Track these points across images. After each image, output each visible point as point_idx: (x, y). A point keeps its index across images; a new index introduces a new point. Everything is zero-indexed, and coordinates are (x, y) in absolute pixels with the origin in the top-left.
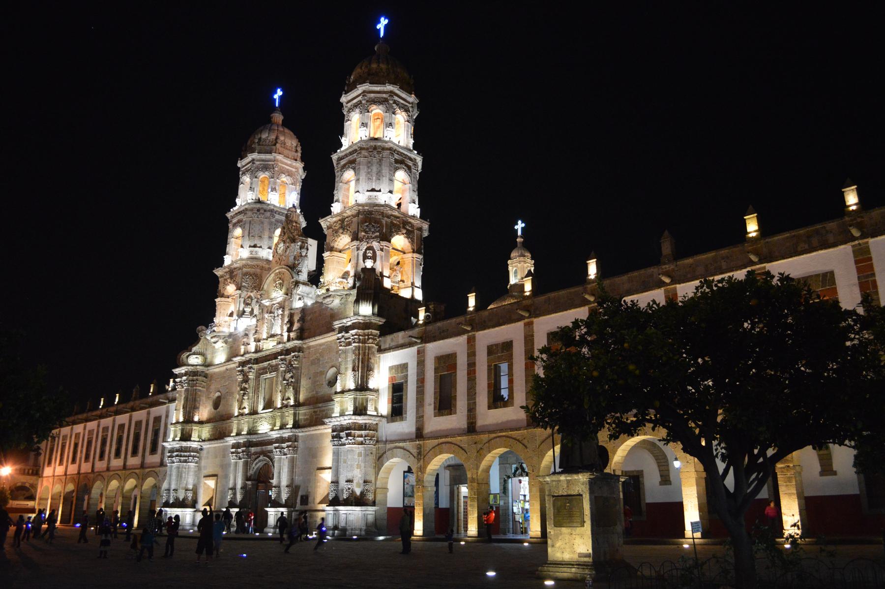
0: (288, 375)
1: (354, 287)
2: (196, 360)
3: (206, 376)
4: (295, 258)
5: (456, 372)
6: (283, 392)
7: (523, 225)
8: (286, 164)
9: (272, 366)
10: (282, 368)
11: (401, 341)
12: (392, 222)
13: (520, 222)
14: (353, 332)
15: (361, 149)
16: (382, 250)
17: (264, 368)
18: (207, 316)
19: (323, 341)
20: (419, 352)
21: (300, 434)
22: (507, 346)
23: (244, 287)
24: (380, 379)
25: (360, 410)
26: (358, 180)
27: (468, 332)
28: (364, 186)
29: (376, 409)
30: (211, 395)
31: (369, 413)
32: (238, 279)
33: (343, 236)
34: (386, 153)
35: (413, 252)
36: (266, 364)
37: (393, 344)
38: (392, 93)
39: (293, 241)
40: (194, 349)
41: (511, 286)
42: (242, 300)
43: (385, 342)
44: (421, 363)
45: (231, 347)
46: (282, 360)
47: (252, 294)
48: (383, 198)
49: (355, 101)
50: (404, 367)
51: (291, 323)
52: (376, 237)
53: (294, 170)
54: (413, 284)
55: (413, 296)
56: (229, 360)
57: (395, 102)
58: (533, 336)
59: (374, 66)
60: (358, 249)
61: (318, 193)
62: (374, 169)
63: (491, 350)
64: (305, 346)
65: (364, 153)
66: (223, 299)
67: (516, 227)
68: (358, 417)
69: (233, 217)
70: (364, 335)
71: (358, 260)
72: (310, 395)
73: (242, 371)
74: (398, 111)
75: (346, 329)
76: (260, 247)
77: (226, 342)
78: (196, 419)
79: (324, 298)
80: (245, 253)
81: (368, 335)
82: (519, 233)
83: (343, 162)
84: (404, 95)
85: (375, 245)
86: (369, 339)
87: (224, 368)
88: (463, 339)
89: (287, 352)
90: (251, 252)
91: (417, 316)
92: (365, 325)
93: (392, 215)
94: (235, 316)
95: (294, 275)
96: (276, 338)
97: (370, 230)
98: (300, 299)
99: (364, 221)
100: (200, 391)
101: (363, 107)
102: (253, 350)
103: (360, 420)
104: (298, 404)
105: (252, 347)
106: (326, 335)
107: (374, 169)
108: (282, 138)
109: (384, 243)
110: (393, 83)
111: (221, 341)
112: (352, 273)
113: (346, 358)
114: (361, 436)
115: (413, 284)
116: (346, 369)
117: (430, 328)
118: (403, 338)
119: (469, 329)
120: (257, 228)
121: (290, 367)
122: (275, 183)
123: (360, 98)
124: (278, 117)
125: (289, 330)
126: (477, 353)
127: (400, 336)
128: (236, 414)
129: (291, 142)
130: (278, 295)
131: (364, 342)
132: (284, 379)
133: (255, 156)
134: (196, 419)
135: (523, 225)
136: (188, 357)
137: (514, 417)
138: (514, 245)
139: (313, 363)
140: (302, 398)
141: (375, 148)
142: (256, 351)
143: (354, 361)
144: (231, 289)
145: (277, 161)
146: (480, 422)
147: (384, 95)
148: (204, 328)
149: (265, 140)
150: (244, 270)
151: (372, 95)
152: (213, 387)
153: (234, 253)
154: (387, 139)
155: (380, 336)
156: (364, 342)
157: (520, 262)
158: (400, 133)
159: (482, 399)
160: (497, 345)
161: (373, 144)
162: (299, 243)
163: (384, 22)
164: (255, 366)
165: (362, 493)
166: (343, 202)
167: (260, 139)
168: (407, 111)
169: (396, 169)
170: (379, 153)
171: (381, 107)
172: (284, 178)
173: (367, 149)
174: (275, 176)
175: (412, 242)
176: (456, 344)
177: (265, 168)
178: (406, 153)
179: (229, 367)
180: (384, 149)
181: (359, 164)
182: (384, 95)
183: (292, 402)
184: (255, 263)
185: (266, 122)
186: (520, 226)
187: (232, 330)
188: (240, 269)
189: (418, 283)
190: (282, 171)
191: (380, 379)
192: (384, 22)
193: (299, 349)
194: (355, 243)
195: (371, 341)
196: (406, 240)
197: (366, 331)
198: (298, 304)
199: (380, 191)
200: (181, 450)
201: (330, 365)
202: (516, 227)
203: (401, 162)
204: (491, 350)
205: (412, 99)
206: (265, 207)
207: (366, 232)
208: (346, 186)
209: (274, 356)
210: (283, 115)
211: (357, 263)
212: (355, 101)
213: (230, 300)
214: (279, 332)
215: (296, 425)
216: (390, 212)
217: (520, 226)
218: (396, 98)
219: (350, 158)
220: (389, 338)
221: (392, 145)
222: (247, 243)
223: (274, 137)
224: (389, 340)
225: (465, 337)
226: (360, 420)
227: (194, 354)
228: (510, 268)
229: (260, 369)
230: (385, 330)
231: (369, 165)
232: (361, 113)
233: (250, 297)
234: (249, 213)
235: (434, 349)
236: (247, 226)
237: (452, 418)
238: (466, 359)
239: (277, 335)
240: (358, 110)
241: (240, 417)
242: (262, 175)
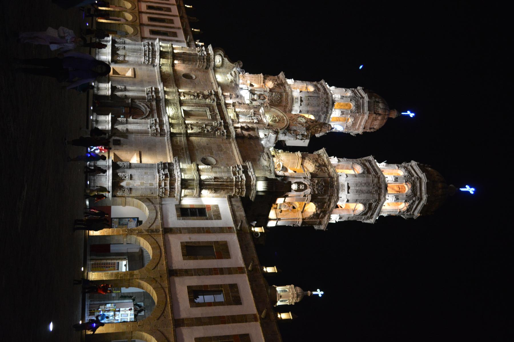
0: (209, 128)
1: (277, 176)
2: (218, 61)
3: (207, 68)
4: (295, 130)
5: (216, 259)
6: (197, 125)
7: (320, 296)
8: (360, 123)
9: (215, 116)
10: (214, 124)
11: (237, 214)
12: (325, 202)
13: (322, 293)
14: (244, 177)
15: (379, 178)
16: (305, 196)
17: (214, 110)
18: (250, 68)
19: (235, 153)
20: (230, 228)
21: (166, 138)
22: (237, 301)
23: (272, 94)
24: (209, 199)
25: (185, 184)
26: (355, 176)
27: (247, 267)
28: (352, 181)
29: (185, 196)
30: (193, 72)
31: (183, 190)
32: (277, 90)
33: (314, 166)
34: (376, 196)
35: (303, 219)
36: (217, 111)
37: (235, 207)
38: (420, 199)
39: (308, 129)
40: (226, 60)
41: (275, 288)
42: (262, 93)
43: (236, 201)
44: (221, 230)
45: (228, 86)
46: (221, 123)
47: (266, 100)
48: (343, 195)
49: (413, 172)
50: (218, 217)
51: (248, 129)
52: (314, 191)
53: (357, 127)
54: (279, 219)
55: (271, 220)
56: (219, 84)
57: (414, 202)
58: (246, 322)
59: (440, 185)
60: (305, 178)
61: (344, 146)
62: (365, 188)
63: (234, 287)
64: (231, 140)
65: (376, 180)
66: (262, 79)
67: (318, 290)
68: (179, 182)
69: (321, 84)
70: (242, 185)
71: (297, 178)
72: (195, 145)
73: (211, 94)
74: (407, 204)
75: (245, 172)
76: (301, 105)
77: (232, 82)
78: (176, 62)
79: (267, 154)
80: (296, 94)
81: (241, 188)
82: (314, 293)
83: (367, 164)
84: (419, 208)
85: (308, 191)
86: (239, 189)
87: (213, 81)
88: (241, 263)
89: (226, 127)
90: (297, 98)
91: (257, 226)
92: (249, 186)
93: (330, 202)
94: (250, 88)
95: (283, 131)
97: (319, 187)
98: (265, 135)
99: (325, 181)
100: (196, 64)
101: (409, 178)
102: (227, 102)
103: (178, 184)
104: (188, 136)
105: (229, 101)
106: (240, 155)
107: (365, 188)
108: (380, 118)
109: (310, 197)
110: (428, 199)
111: (232, 78)
112: (286, 174)
113: (224, 172)
114: (165, 185)
115: (279, 219)
116: (216, 172)
117: (249, 236)
118: (240, 215)
119: (250, 268)
120: (315, 102)
121: (215, 129)
122: (347, 114)
123: (415, 175)
124: (394, 115)
125: (242, 128)
126: (231, 275)
127: (241, 213)
128: (180, 90)
129: (377, 125)
130: (267, 119)
131: (236, 185)
132: (206, 125)
133: (366, 99)
134: (176, 62)
135: (320, 296)
136: (220, 55)
137: (182, 308)
138: (305, 289)
139: (219, 146)
140: (193, 139)
141: (380, 188)
142: (227, 105)
143: (222, 178)
144: (270, 84)
145: (363, 115)
146: (177, 280)
147: (418, 193)
148: (241, 66)
149: (378, 106)
150: (284, 94)
151: (418, 185)
152: (199, 73)
153: (296, 86)
154: (387, 197)
155: (241, 197)
156: (236, 185)
157: (293, 294)
158: (391, 206)
159: (195, 281)
160: (238, 292)
161: (383, 186)
162: (306, 133)
163: (471, 190)
164: (215, 104)
165: (122, 187)
166: (338, 165)
167: (378, 102)
168: (408, 210)
169: (365, 205)
170: (376, 191)
171: (410, 191)
172: (351, 120)
173: (379, 182)
174: (353, 114)
175: (310, 218)
176: (237, 258)
177: (359, 107)
178: (377, 211)
179: (214, 84)
180: (379, 195)
181: (368, 177)
182: (418, 193)
183: (189, 131)
184: (290, 101)
185: (390, 106)
186: (319, 293)
187: (241, 86)
188: (285, 91)
189: (280, 223)
190: (356, 119)
191: (209, 199)
192: (471, 190)
193: (229, 135)
194: (309, 176)
195: (237, 190)
196: (312, 213)
197: (245, 187)
198: (261, 134)
199: (348, 193)
200: (154, 52)
201: (218, 159)
202: (318, 290)
203: (371, 207)
204: (234, 287)
205: (417, 214)
206: (330, 107)
207: (317, 184)
208: (350, 167)
209: (223, 117)
210: (396, 118)
211: (294, 178)
212: (413, 172)
213: (262, 84)
214: (241, 120)
215: (172, 135)
216: (333, 201)
217: (319, 293)
218: (417, 202)
219: (371, 170)
220: (239, 204)
221: (382, 200)
222: (303, 95)
223: (380, 111)
224: (238, 204)
225: (243, 265)
226: (178, 184)
227: (223, 60)
228: (288, 287)
229: (213, 107)
230: (246, 202)
231: (367, 184)
232: (405, 177)
233: (265, 98)
234: (325, 96)
235: (233, 240)
236: (316, 95)
237: (181, 257)
238: (226, 267)
239: (238, 119)
240: (406, 174)
241: (177, 93)
242: (352, 105)
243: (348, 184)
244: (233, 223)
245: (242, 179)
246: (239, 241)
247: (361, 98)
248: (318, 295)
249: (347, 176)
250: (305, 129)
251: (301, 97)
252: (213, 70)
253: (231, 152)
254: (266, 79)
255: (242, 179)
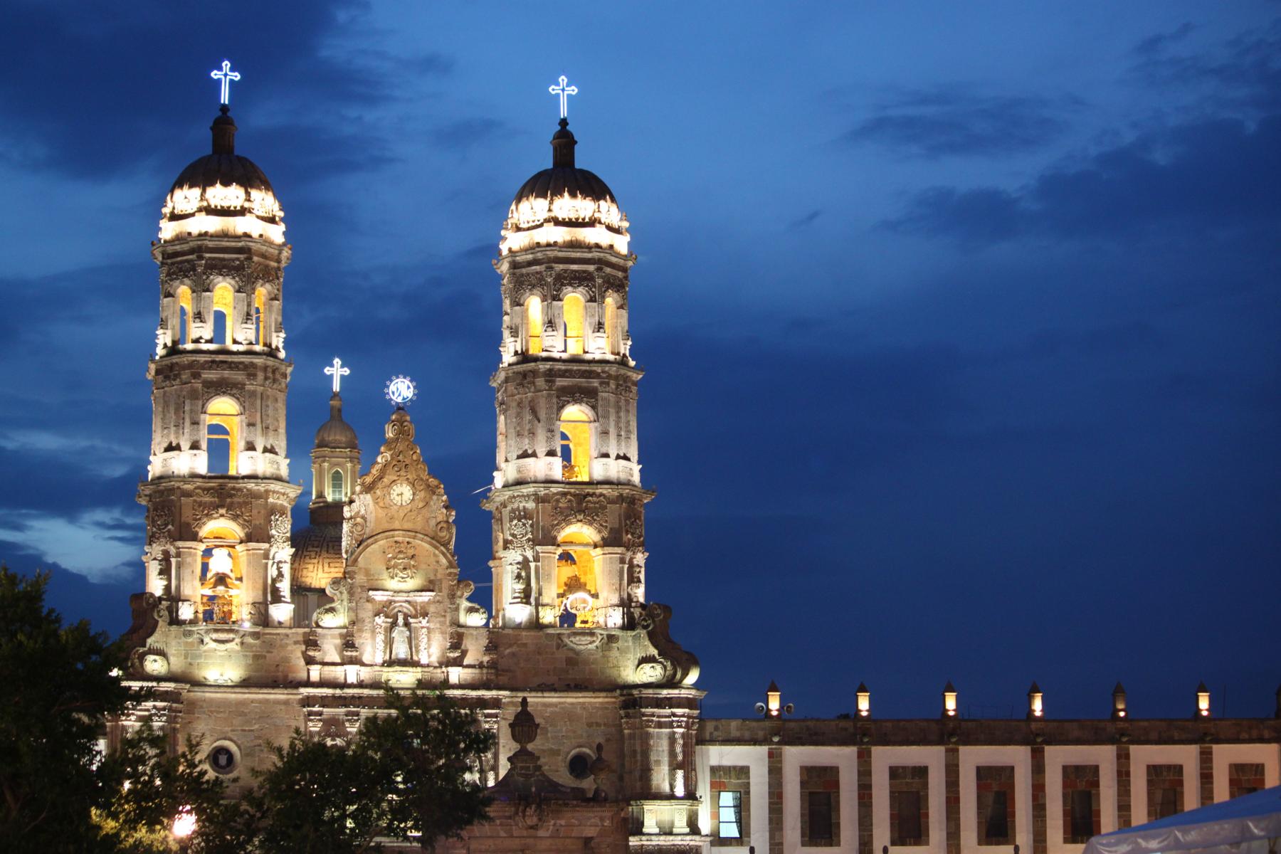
5: (838, 792)
7: (347, 371)
11: (735, 733)
14: (679, 711)
20: (771, 755)
39: (432, 490)
40: (149, 641)
45: (256, 657)
49: (575, 267)
58: (957, 766)
60: (622, 561)
83: (560, 382)
96: (419, 669)
123: (591, 268)
136: (142, 658)
151: (608, 270)
173: (617, 378)
234: (261, 376)
235: (796, 756)
243: (618, 457)
244: (758, 748)
245: (683, 716)
246: (803, 744)
247: (250, 259)
248: (342, 376)
249: (606, 455)
250: (435, 497)
251: (265, 450)
252: (196, 689)
253: (549, 710)
254: (197, 533)
255: (683, 716)
